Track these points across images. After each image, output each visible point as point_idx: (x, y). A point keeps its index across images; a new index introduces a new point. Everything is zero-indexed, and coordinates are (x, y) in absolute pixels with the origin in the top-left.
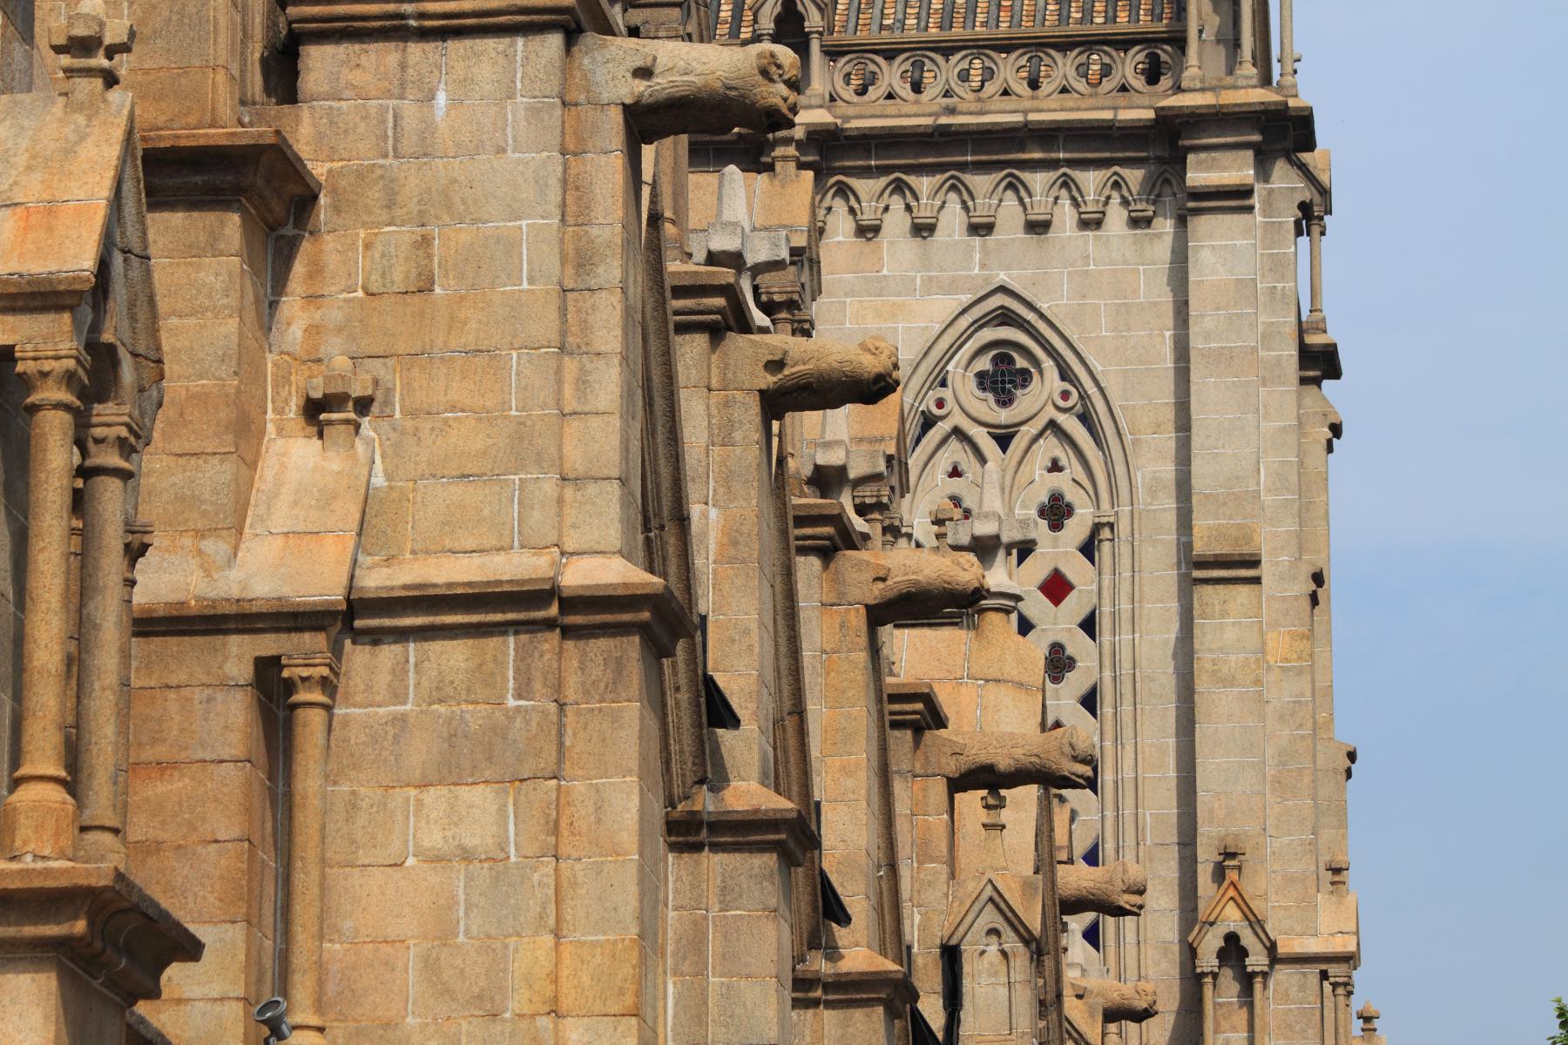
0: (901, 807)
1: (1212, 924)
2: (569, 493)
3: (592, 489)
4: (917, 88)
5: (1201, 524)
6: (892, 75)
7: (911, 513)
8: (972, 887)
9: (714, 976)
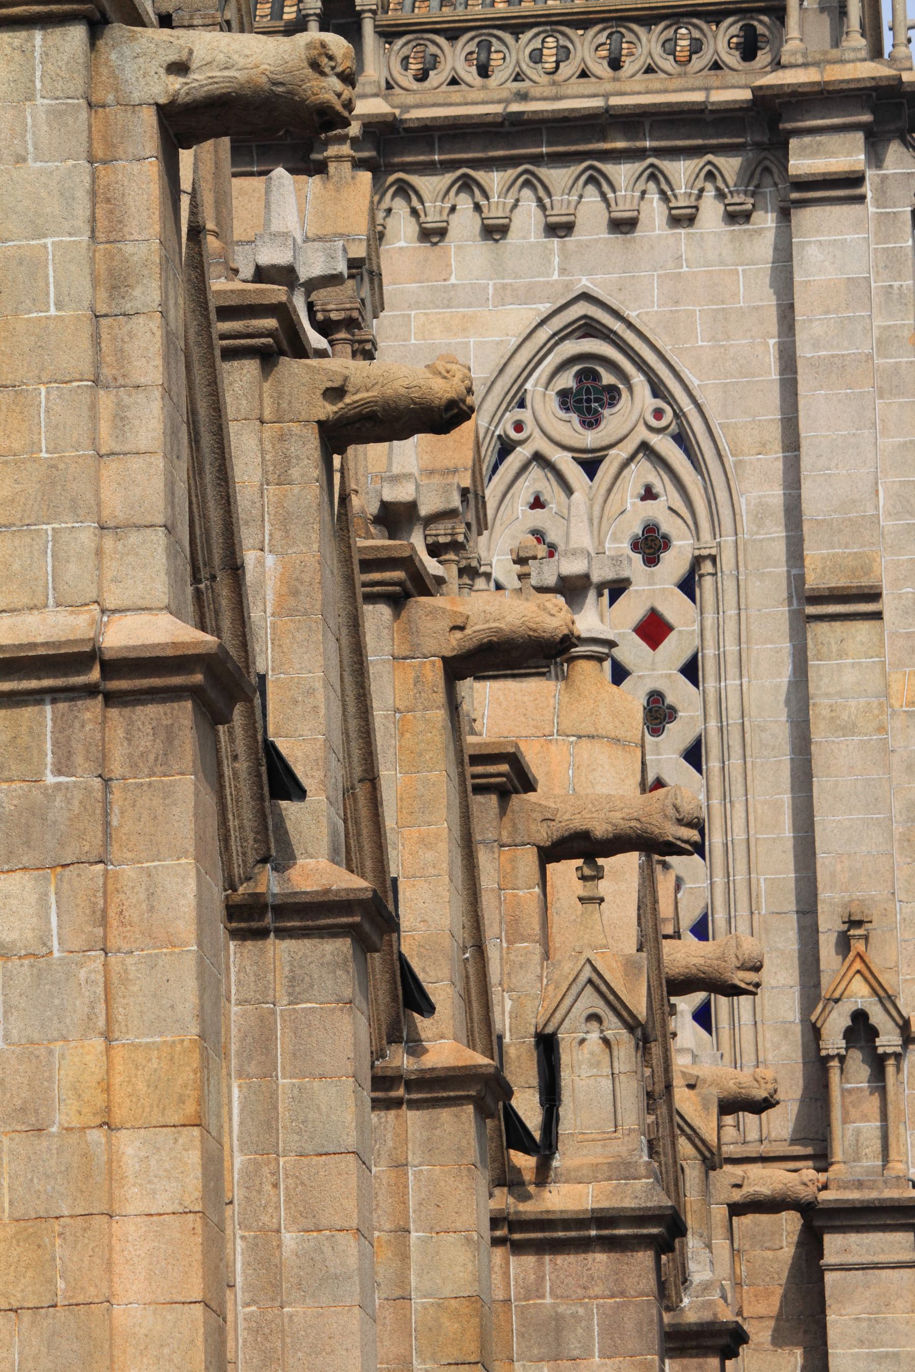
0: (488, 880)
1: (837, 1001)
2: (109, 543)
3: (134, 538)
4: (484, 71)
5: (813, 554)
7: (489, 550)
8: (568, 968)
9: (284, 1077)
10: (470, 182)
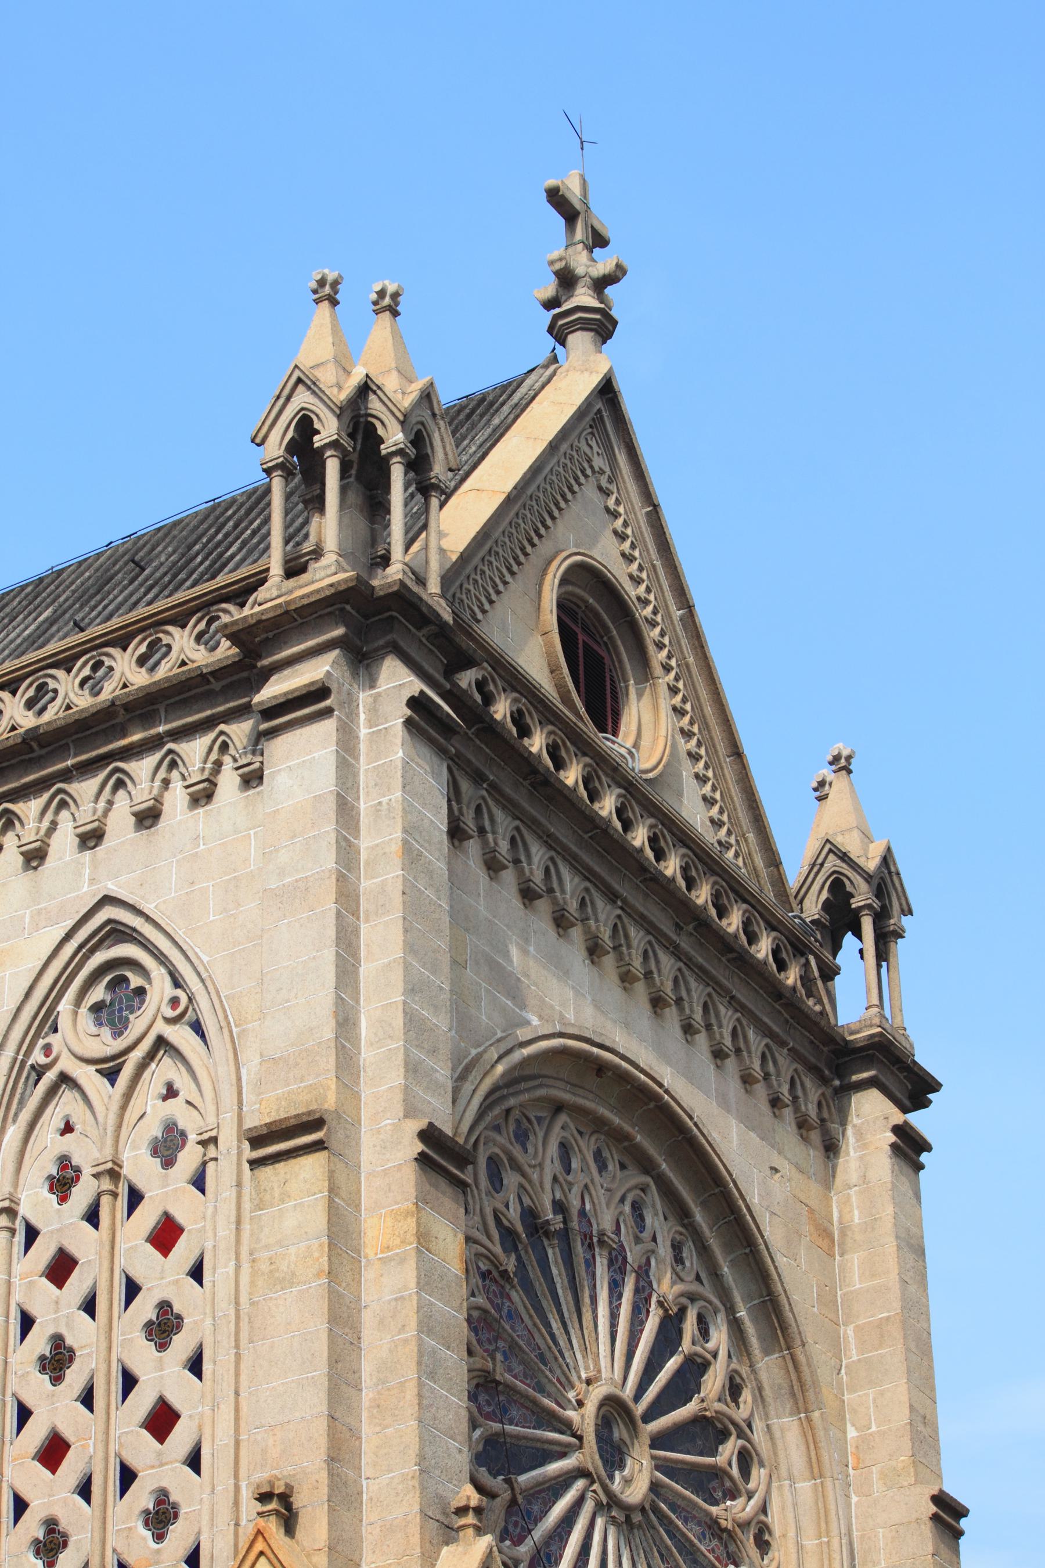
10: (12, 817)
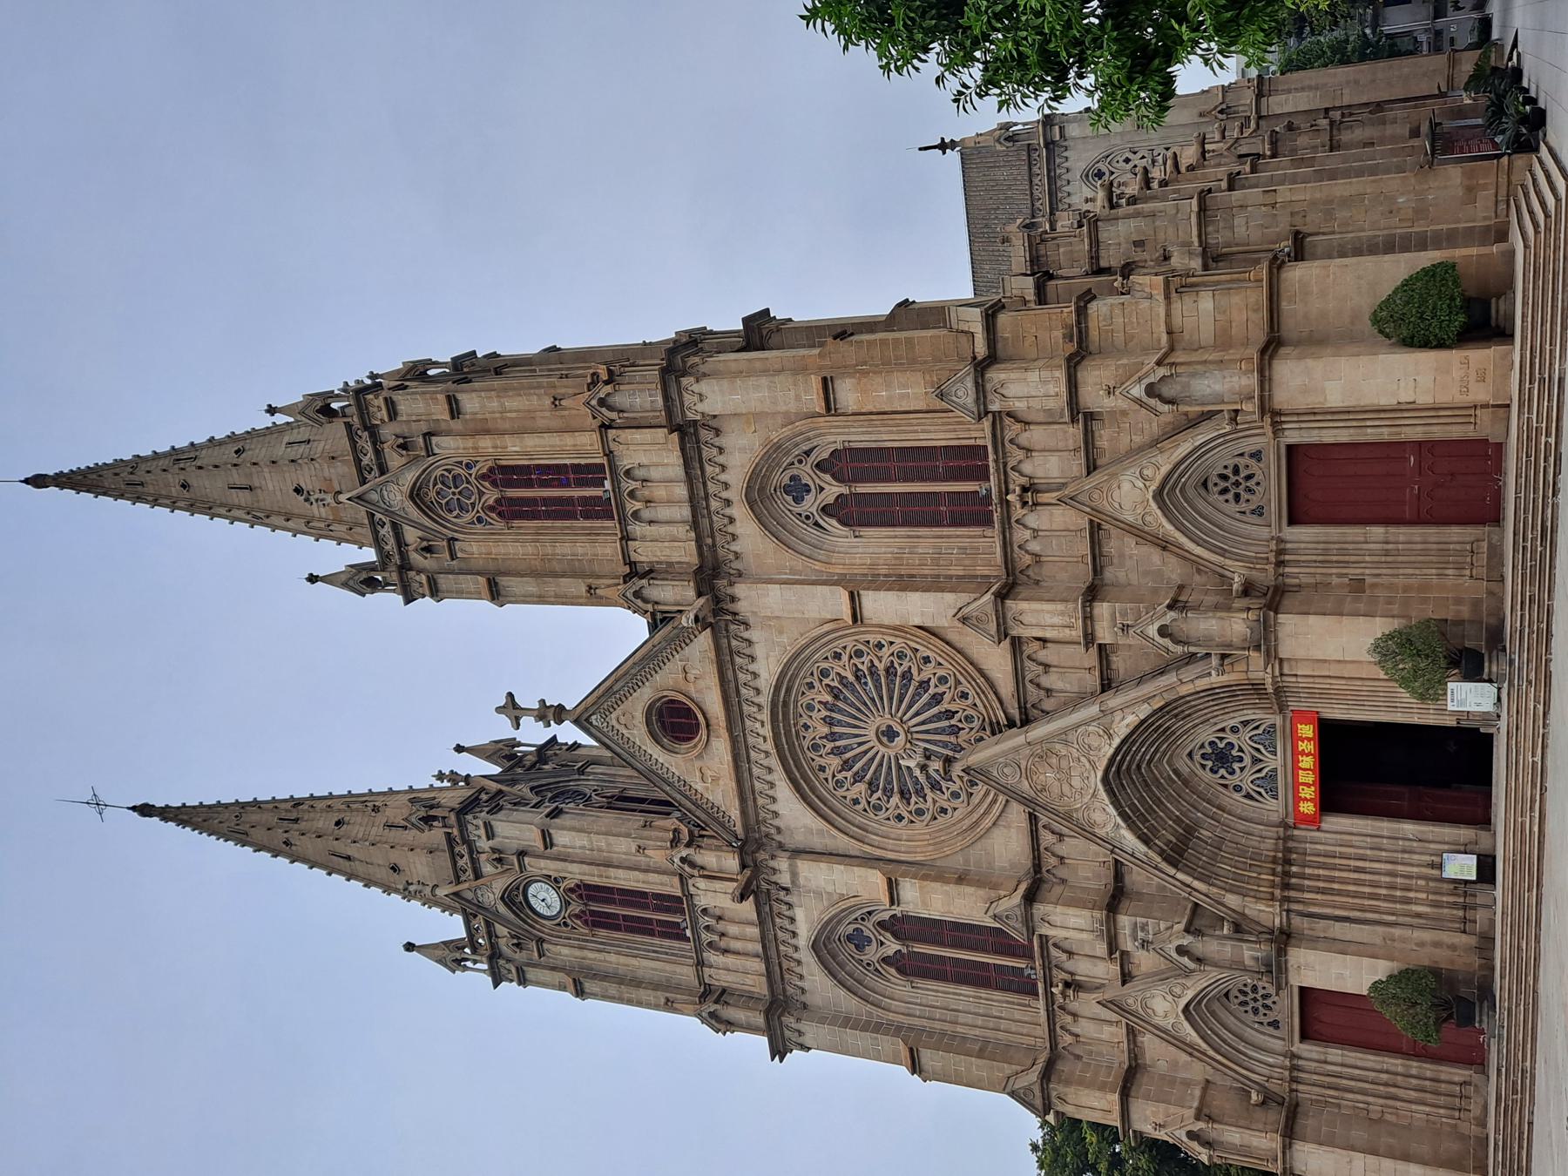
6: (1038, 204)
